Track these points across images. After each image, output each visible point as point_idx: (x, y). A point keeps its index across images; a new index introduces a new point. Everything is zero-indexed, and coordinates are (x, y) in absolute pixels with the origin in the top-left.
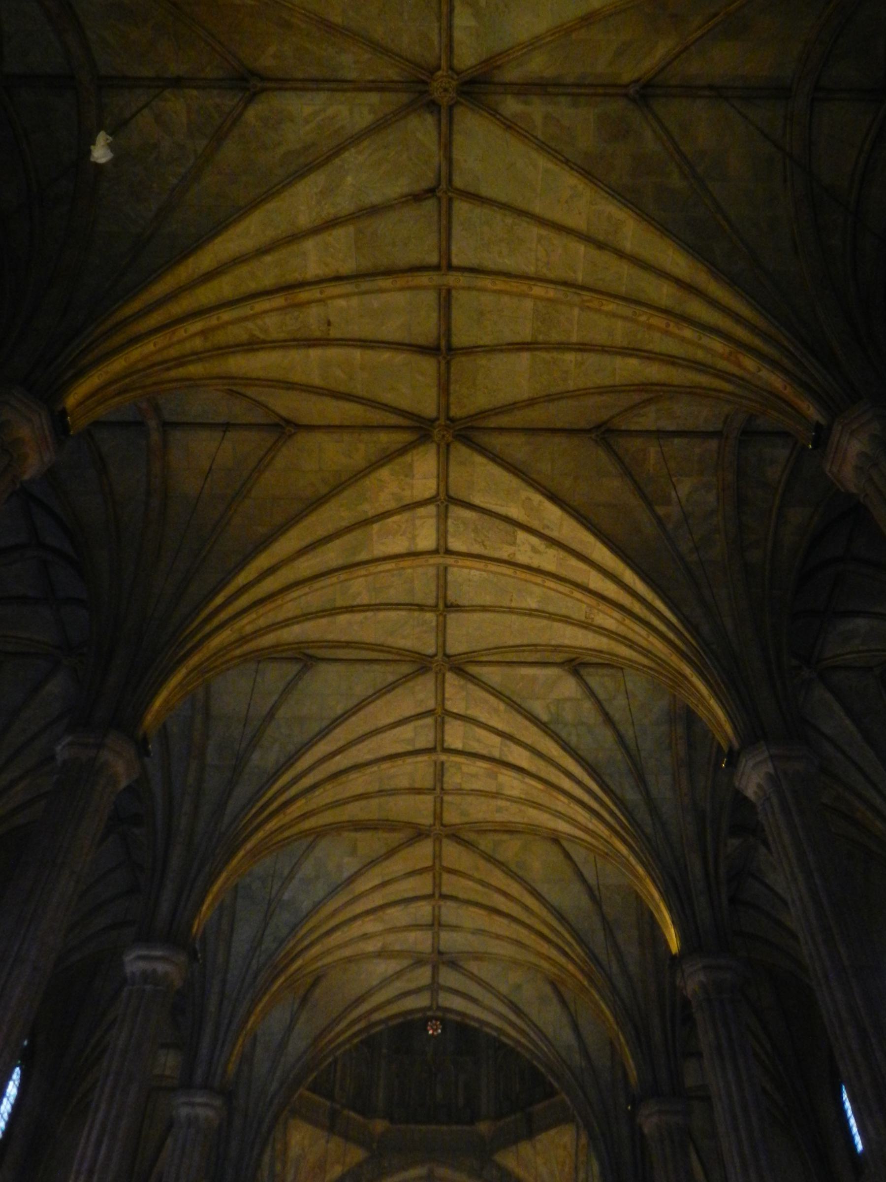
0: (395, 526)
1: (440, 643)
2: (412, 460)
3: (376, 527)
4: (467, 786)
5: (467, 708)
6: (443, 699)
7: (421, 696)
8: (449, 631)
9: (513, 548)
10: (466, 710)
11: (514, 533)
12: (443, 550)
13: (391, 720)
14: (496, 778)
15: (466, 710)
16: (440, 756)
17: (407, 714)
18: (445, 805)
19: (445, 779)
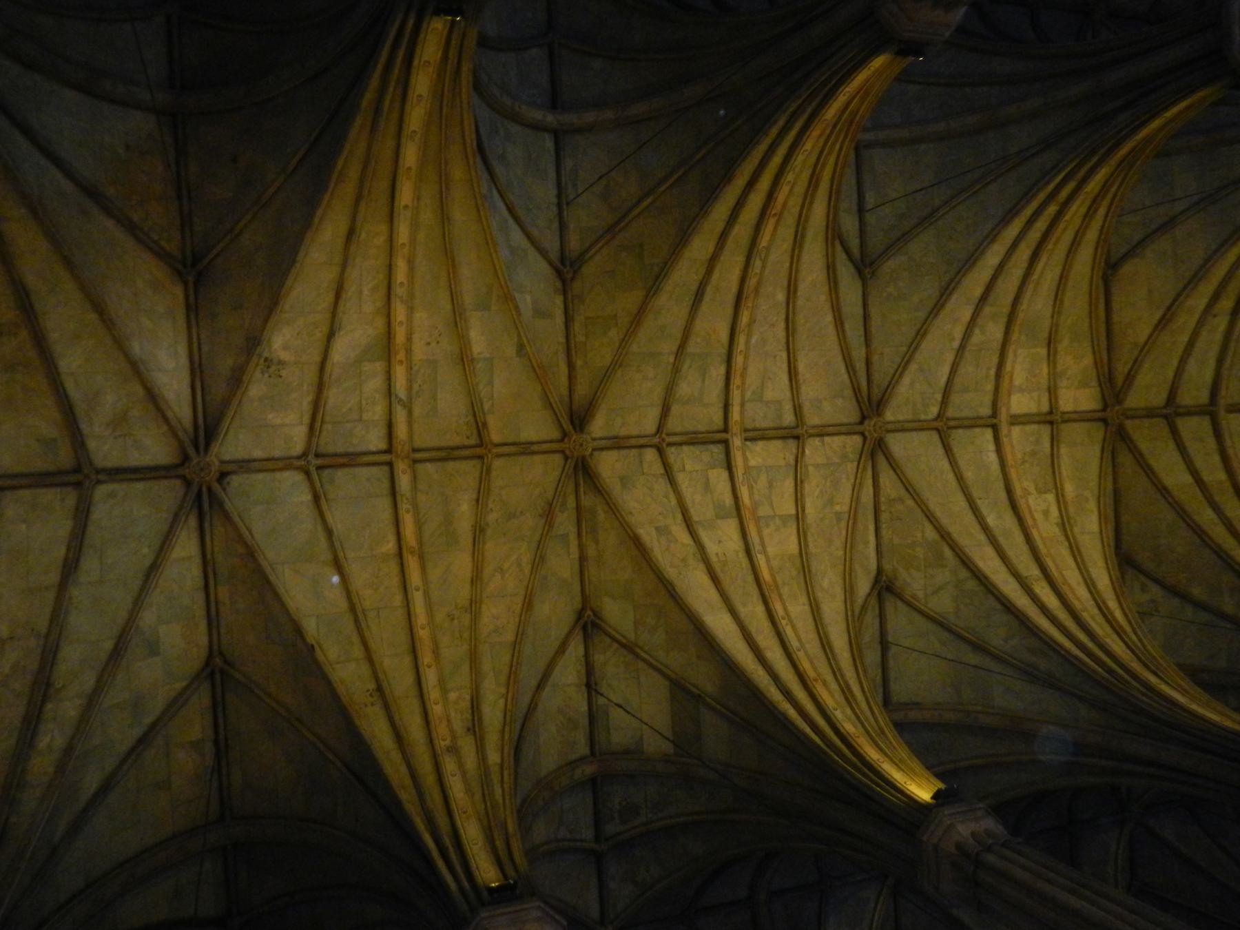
0: (1037, 371)
1: (907, 425)
2: (1090, 387)
3: (1044, 351)
4: (681, 478)
5: (817, 466)
6: (821, 435)
7: (827, 406)
8: (914, 434)
9: (1034, 492)
10: (813, 465)
11: (1049, 490)
12: (387, 457)
13: (801, 367)
14: (719, 517)
15: (813, 465)
16: (739, 437)
17: (804, 389)
18: (634, 452)
19: (685, 448)
